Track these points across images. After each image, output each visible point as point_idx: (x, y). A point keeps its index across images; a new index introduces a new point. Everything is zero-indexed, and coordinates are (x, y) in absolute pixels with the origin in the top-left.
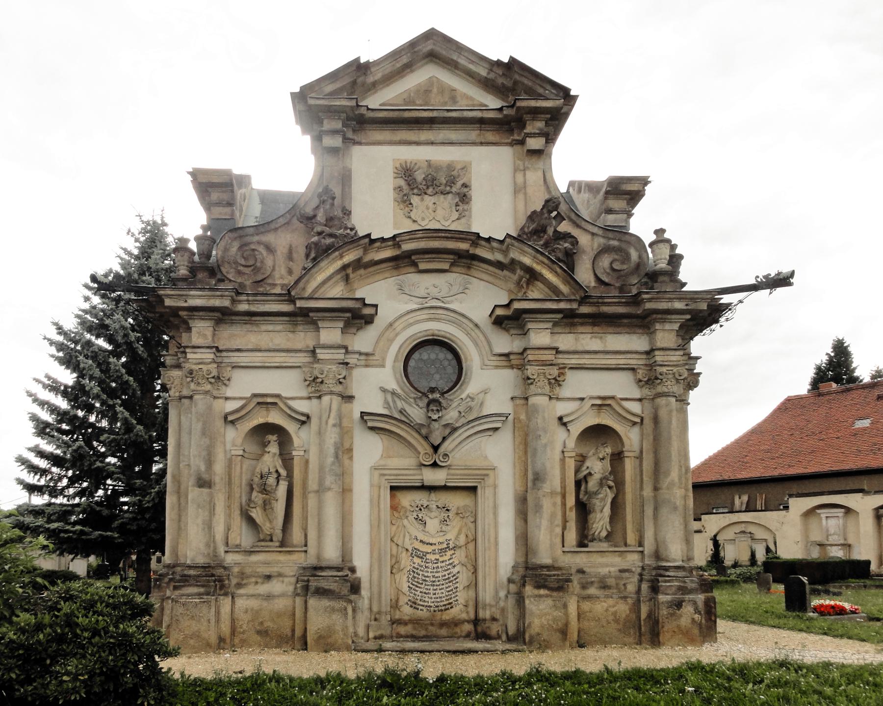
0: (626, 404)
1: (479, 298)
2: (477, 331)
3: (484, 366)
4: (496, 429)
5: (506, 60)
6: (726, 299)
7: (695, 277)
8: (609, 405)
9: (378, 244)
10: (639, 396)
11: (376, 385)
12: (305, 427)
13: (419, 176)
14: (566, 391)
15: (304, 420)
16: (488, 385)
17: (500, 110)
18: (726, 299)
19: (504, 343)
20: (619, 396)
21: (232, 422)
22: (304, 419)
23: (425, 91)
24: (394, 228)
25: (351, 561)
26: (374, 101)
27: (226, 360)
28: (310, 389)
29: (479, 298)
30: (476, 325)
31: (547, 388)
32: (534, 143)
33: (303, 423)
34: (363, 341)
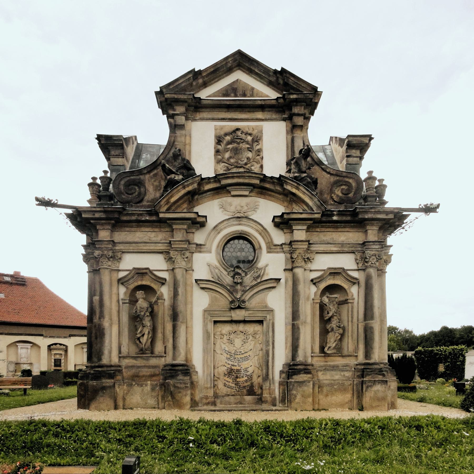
5: (279, 69)
7: (392, 200)
11: (205, 264)
16: (272, 264)
19: (279, 237)
23: (232, 89)
27: (117, 248)
34: (199, 237)
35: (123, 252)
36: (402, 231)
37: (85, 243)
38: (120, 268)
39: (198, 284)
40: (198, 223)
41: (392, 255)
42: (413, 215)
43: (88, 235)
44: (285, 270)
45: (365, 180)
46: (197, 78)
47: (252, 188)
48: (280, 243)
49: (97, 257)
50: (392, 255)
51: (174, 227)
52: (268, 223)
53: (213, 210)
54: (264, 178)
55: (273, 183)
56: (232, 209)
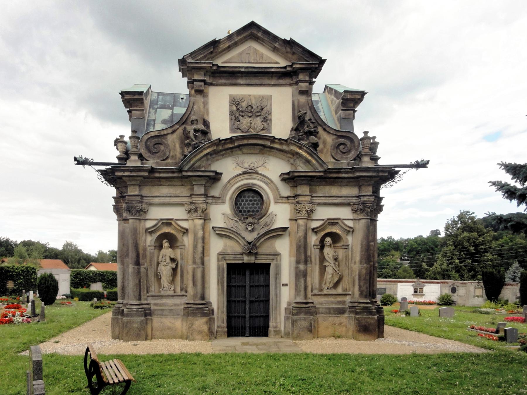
0: (345, 222)
1: (274, 168)
2: (272, 184)
3: (276, 203)
4: (281, 235)
5: (288, 39)
6: (397, 169)
8: (337, 223)
9: (223, 142)
10: (352, 218)
12: (186, 235)
13: (244, 104)
14: (316, 216)
15: (186, 231)
17: (285, 67)
18: (397, 169)
19: (285, 191)
20: (342, 218)
21: (149, 232)
22: (185, 231)
24: (231, 133)
25: (209, 299)
26: (219, 62)
27: (144, 201)
28: (189, 215)
29: (274, 168)
30: (272, 181)
31: (307, 215)
32: (304, 86)
33: (184, 233)
34: (215, 192)
35: (150, 204)
36: (392, 183)
37: (115, 196)
38: (147, 218)
39: (215, 231)
40: (216, 177)
41: (383, 205)
42: (403, 170)
43: (117, 188)
44: (290, 220)
45: (361, 140)
46: (213, 47)
47: (262, 147)
48: (286, 195)
49: (127, 208)
50: (383, 205)
51: (194, 183)
52: (275, 177)
53: (229, 168)
54: (273, 140)
55: (281, 144)
56: (246, 165)
